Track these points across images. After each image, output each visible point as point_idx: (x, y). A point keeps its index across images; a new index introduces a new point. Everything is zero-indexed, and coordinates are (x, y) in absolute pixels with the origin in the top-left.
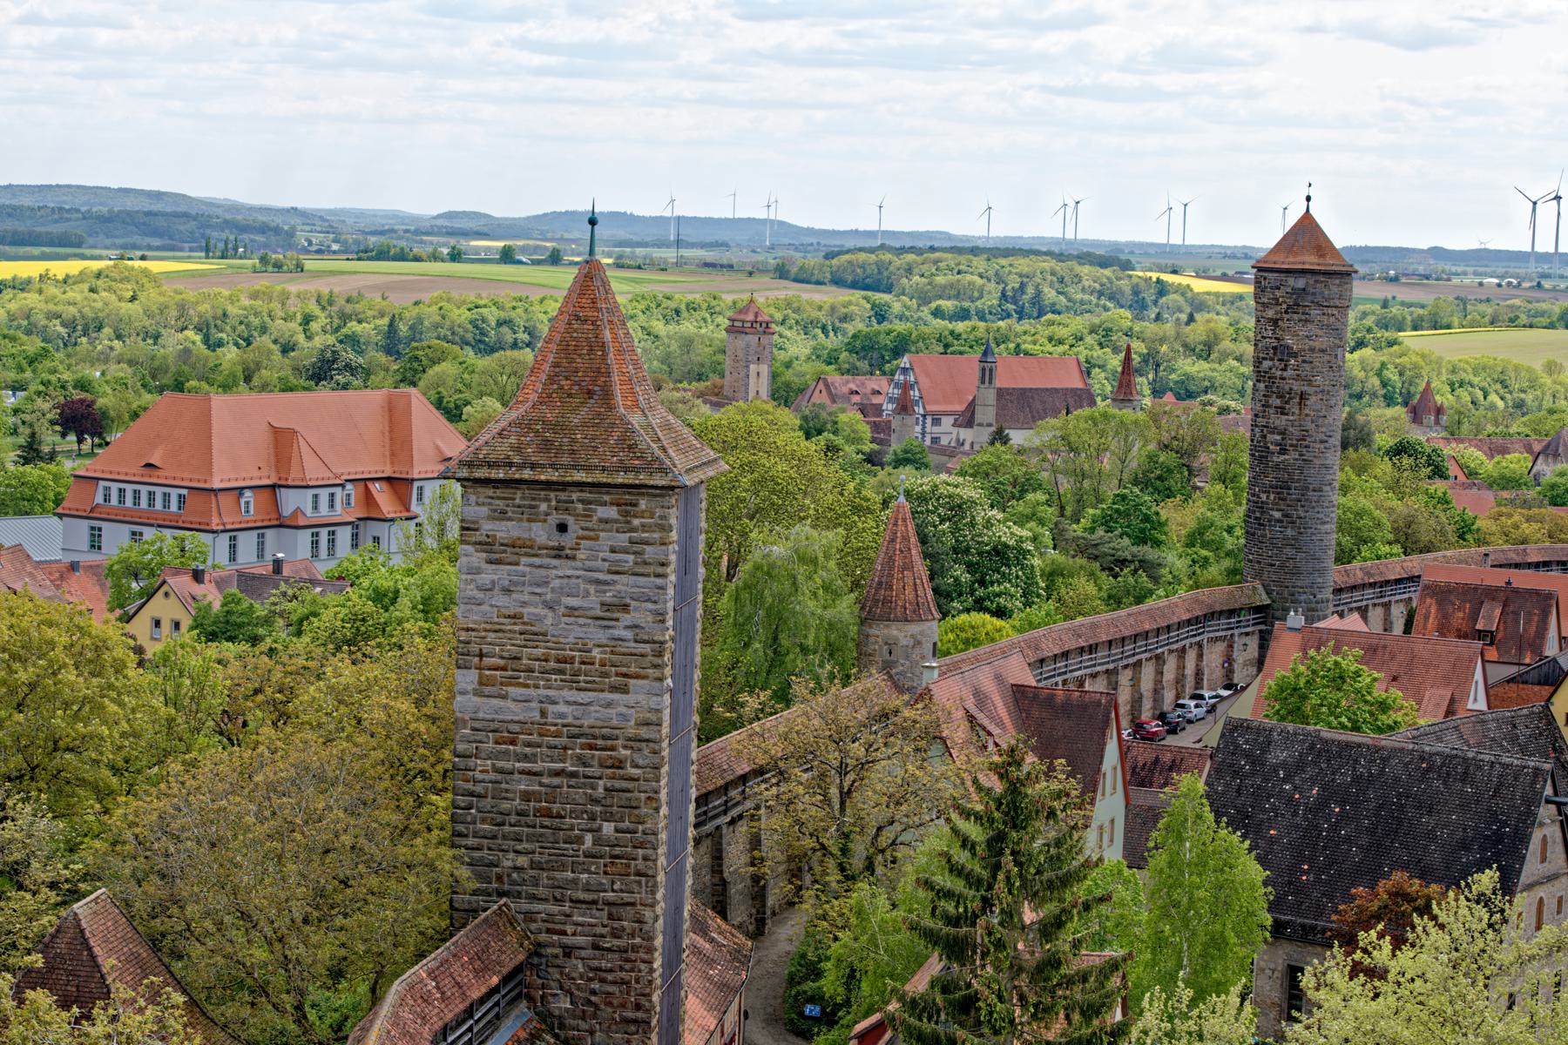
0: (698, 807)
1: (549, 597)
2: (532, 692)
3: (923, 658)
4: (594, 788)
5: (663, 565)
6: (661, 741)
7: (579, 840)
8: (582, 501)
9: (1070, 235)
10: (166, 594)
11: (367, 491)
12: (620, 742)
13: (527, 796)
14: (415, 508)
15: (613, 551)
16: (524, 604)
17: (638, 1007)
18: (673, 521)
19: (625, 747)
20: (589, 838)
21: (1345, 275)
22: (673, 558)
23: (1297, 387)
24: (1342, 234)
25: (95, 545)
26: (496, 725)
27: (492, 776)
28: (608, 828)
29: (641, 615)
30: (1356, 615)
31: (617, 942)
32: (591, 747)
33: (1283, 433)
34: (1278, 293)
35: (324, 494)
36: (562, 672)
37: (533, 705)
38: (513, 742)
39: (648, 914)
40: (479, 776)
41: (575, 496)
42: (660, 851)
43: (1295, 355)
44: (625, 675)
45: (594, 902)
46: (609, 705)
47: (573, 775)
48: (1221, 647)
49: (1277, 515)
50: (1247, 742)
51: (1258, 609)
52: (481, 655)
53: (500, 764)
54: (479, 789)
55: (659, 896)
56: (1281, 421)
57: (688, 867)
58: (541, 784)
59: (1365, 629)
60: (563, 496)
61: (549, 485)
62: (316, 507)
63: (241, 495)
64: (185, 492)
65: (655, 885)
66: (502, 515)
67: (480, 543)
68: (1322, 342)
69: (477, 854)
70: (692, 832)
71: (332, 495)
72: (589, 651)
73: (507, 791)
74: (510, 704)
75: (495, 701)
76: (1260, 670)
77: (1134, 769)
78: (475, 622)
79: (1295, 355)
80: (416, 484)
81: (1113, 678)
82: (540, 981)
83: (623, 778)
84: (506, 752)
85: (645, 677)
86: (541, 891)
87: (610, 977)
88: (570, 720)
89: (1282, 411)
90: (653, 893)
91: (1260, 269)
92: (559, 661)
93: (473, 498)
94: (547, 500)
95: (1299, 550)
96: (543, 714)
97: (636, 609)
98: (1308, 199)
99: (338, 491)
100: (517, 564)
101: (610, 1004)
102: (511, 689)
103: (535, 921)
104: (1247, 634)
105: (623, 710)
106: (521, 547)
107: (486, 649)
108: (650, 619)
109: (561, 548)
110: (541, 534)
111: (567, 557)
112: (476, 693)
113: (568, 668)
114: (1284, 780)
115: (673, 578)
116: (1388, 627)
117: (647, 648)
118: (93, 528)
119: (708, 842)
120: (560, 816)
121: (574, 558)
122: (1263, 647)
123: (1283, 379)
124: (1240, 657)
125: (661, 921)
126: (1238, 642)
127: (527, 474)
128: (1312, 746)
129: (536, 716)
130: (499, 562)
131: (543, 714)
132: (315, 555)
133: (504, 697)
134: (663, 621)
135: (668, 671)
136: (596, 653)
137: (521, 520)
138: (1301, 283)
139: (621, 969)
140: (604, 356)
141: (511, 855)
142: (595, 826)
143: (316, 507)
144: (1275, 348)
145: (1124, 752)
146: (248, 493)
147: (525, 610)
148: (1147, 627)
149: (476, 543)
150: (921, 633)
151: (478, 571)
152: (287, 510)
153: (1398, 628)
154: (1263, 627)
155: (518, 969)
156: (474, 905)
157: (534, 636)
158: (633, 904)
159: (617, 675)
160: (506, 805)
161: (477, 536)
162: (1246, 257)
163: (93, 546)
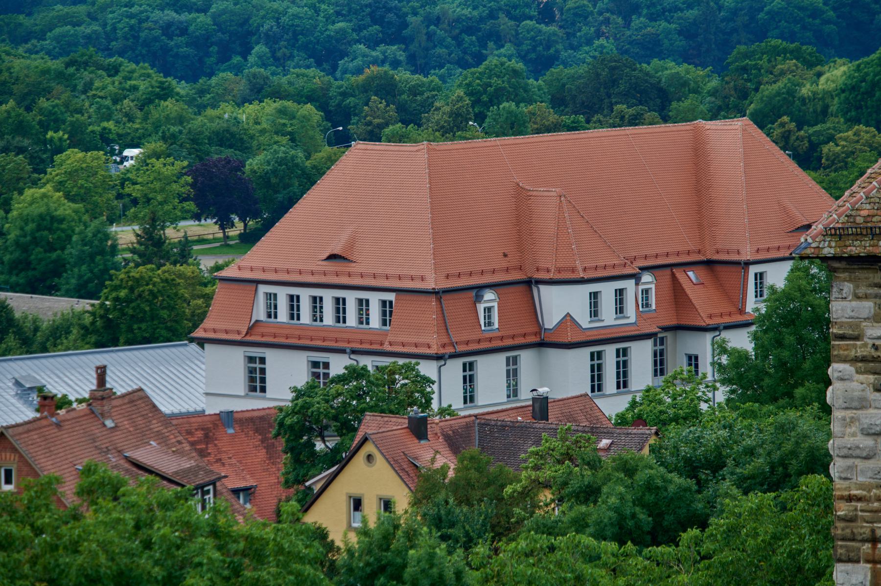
10: (370, 458)
25: (257, 381)
35: (607, 290)
62: (594, 312)
63: (479, 298)
64: (391, 297)
67: (864, 360)
71: (620, 293)
78: (861, 486)
99: (629, 285)
118: (251, 359)
132: (597, 384)
143: (594, 312)
146: (489, 295)
149: (855, 360)
151: (863, 404)
152: (551, 319)
161: (860, 349)
163: (253, 389)
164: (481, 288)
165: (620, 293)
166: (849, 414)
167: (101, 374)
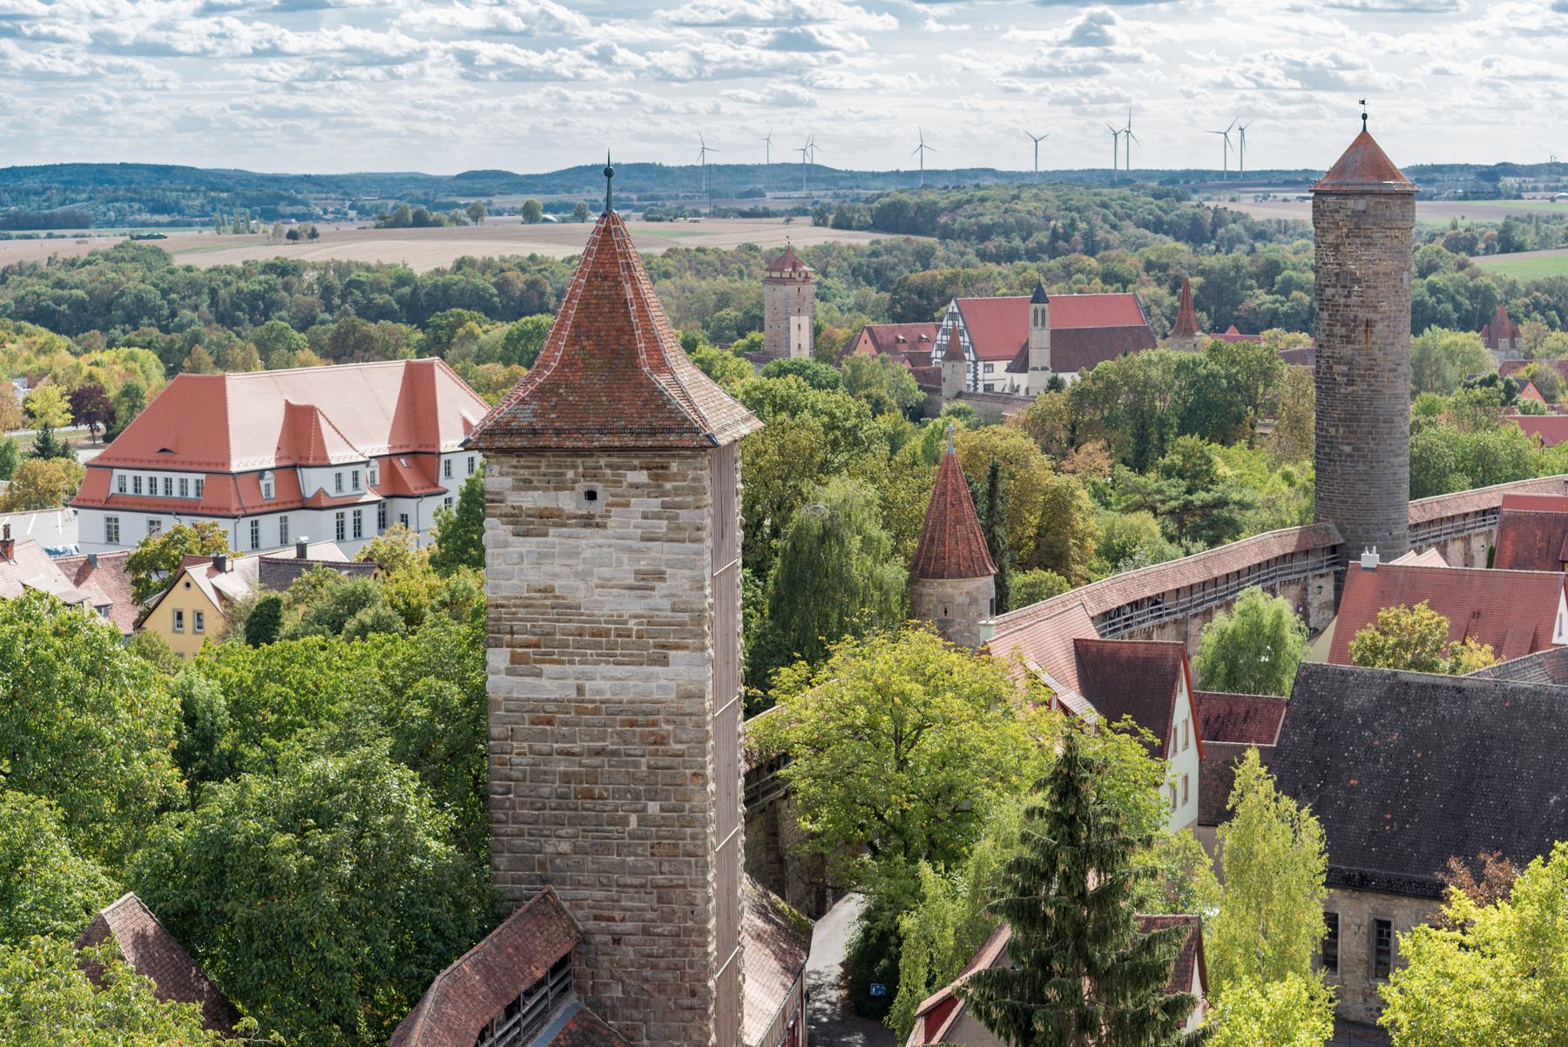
0: (747, 784)
1: (580, 568)
2: (567, 667)
3: (981, 615)
4: (636, 765)
5: (698, 529)
6: (705, 713)
7: (624, 822)
8: (610, 466)
9: (1122, 166)
10: (188, 585)
11: (392, 465)
12: (661, 717)
13: (566, 778)
14: (443, 482)
15: (645, 517)
16: (555, 576)
17: (693, 993)
18: (707, 483)
19: (668, 722)
20: (633, 819)
21: (1407, 196)
22: (708, 521)
23: (1363, 314)
24: (1402, 154)
25: (112, 535)
26: (532, 705)
27: (529, 759)
28: (653, 808)
29: (678, 581)
30: (1433, 551)
31: (666, 928)
32: (632, 724)
33: (1349, 363)
34: (1337, 216)
36: (598, 646)
37: (568, 682)
38: (550, 722)
39: (699, 895)
40: (516, 760)
41: (602, 462)
42: (710, 830)
43: (1358, 281)
44: (664, 647)
45: (643, 886)
46: (647, 679)
47: (615, 753)
48: (1294, 590)
49: (1347, 449)
50: (1322, 688)
51: (1334, 549)
52: (512, 633)
53: (539, 746)
54: (514, 774)
55: (710, 877)
56: (1347, 351)
57: (740, 844)
58: (580, 765)
59: (1443, 565)
60: (590, 462)
61: (575, 452)
62: (339, 488)
65: (706, 865)
66: (526, 485)
68: (1387, 265)
69: (518, 841)
70: (741, 809)
71: (356, 473)
72: (626, 623)
73: (545, 773)
74: (544, 681)
75: (529, 680)
76: (1336, 613)
77: (1207, 722)
78: (504, 598)
79: (1358, 281)
80: (443, 458)
81: (1183, 628)
82: (589, 971)
83: (665, 754)
84: (544, 732)
85: (686, 648)
86: (585, 877)
87: (662, 963)
88: (608, 696)
89: (1348, 340)
90: (704, 874)
91: (1317, 193)
92: (593, 635)
93: (496, 469)
94: (575, 467)
95: (1371, 485)
96: (580, 690)
97: (672, 576)
98: (1365, 117)
100: (546, 535)
101: (662, 991)
102: (545, 667)
103: (582, 908)
104: (1321, 576)
105: (665, 682)
106: (549, 517)
107: (517, 625)
108: (687, 587)
109: (590, 516)
110: (568, 502)
111: (597, 525)
112: (510, 672)
113: (606, 641)
114: (1364, 727)
115: (709, 543)
116: (1468, 559)
117: (686, 617)
118: (109, 520)
119: (762, 818)
120: (601, 797)
121: (604, 526)
122: (1338, 589)
123: (1347, 306)
124: (1315, 601)
125: (714, 902)
126: (1313, 584)
127: (554, 441)
128: (1391, 688)
129: (573, 694)
130: (526, 534)
131: (580, 690)
133: (539, 675)
134: (702, 588)
135: (708, 641)
136: (632, 624)
137: (547, 489)
138: (1361, 205)
139: (674, 954)
140: (627, 314)
141: (554, 840)
142: (639, 807)
143: (339, 488)
144: (1337, 275)
145: (1196, 702)
146: (268, 475)
147: (556, 583)
148: (1216, 573)
150: (977, 589)
151: (506, 544)
152: (309, 493)
153: (1480, 565)
154: (1338, 568)
155: (564, 961)
156: (518, 894)
157: (567, 609)
158: (684, 886)
159: (656, 646)
160: (545, 790)
161: (504, 508)
162: (1307, 181)
163: (110, 539)
164: (263, 471)
165: (356, 473)
166: (496, 551)
167: (7, 529)
